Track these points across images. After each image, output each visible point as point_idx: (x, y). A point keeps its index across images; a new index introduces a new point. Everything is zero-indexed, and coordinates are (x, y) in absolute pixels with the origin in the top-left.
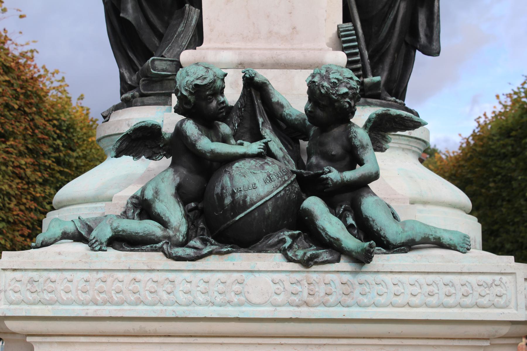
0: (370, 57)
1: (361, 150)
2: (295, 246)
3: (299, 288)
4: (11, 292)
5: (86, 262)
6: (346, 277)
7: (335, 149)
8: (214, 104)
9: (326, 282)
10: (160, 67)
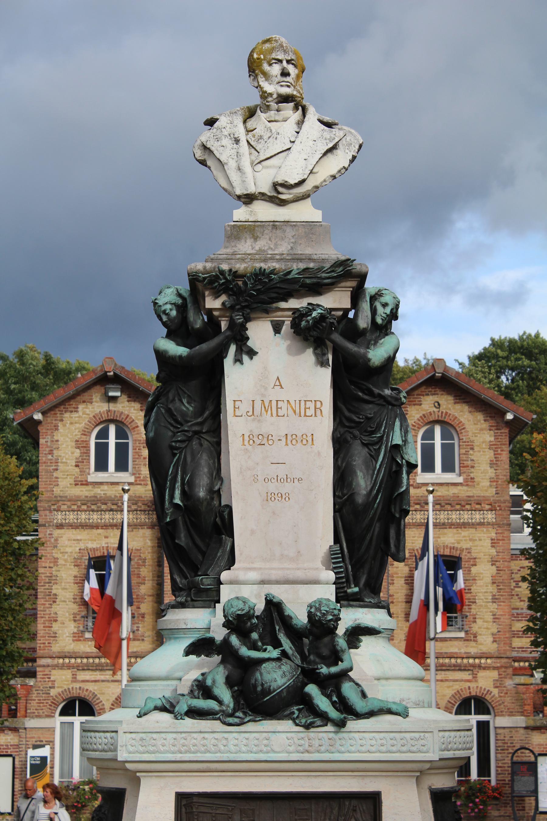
3: (302, 742)
4: (130, 746)
6: (331, 735)
7: (325, 652)
8: (249, 624)
9: (319, 738)
10: (206, 583)
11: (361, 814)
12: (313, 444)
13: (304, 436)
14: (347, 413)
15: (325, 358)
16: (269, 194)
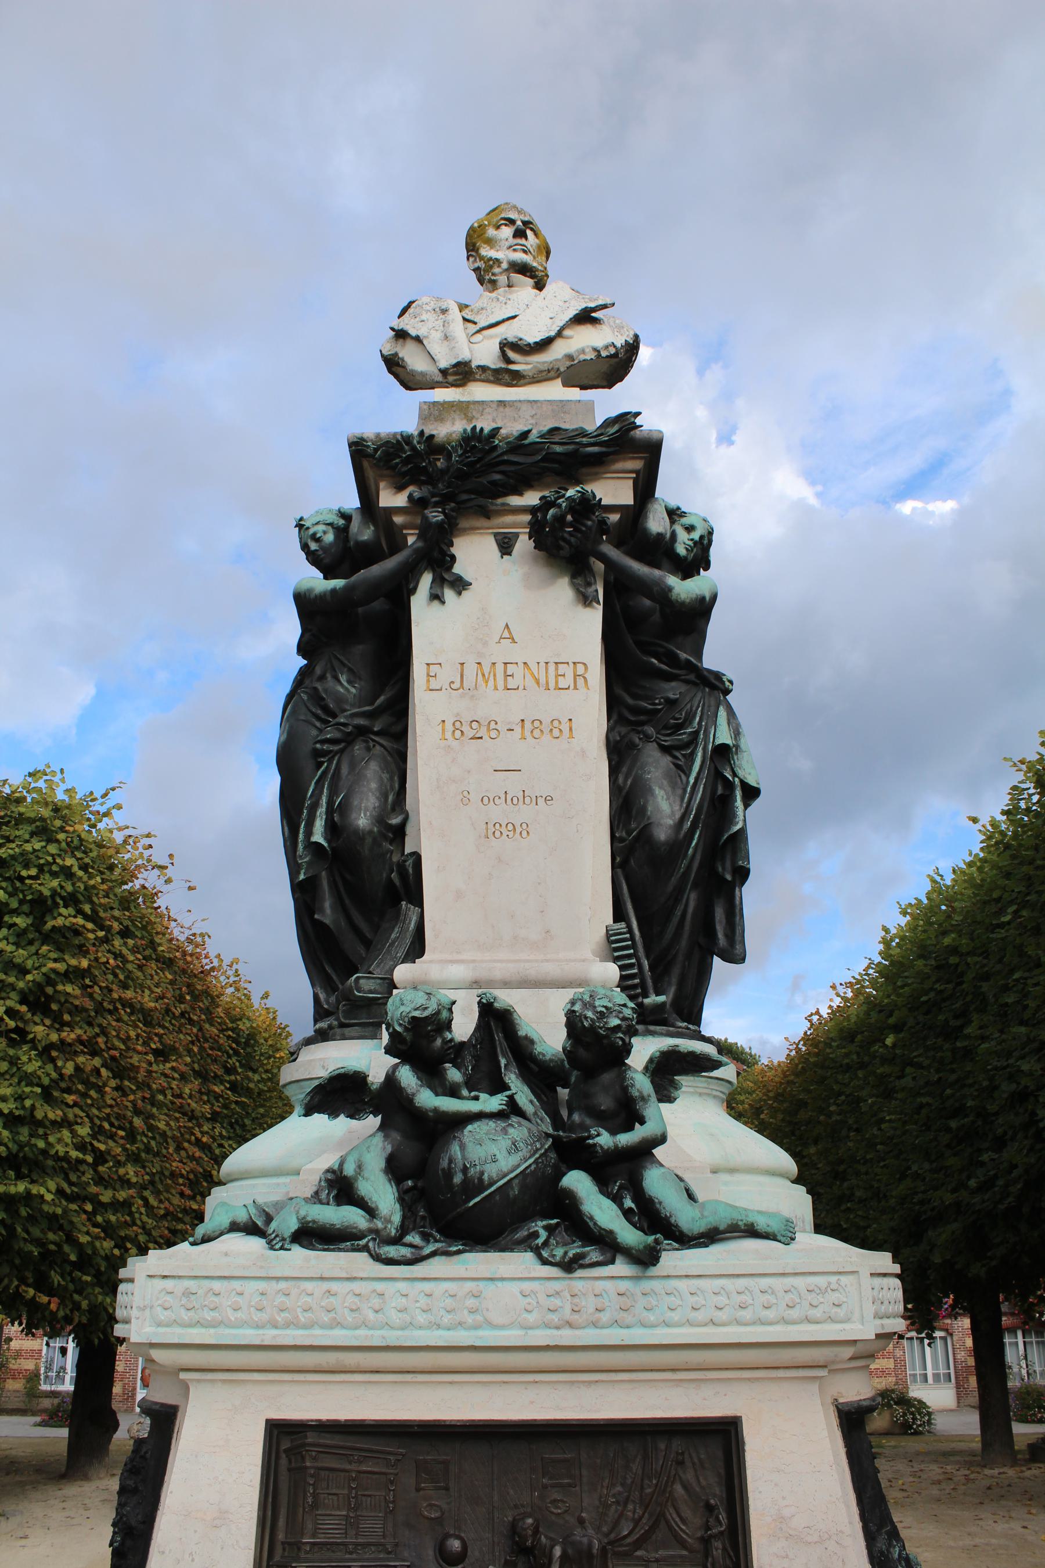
0: (652, 968)
1: (641, 1103)
2: (552, 1241)
3: (558, 1302)
5: (262, 1267)
6: (624, 1285)
8: (439, 1042)
9: (597, 1292)
10: (366, 988)
11: (695, 1470)
13: (556, 723)
14: (630, 701)
15: (591, 590)
16: (493, 367)
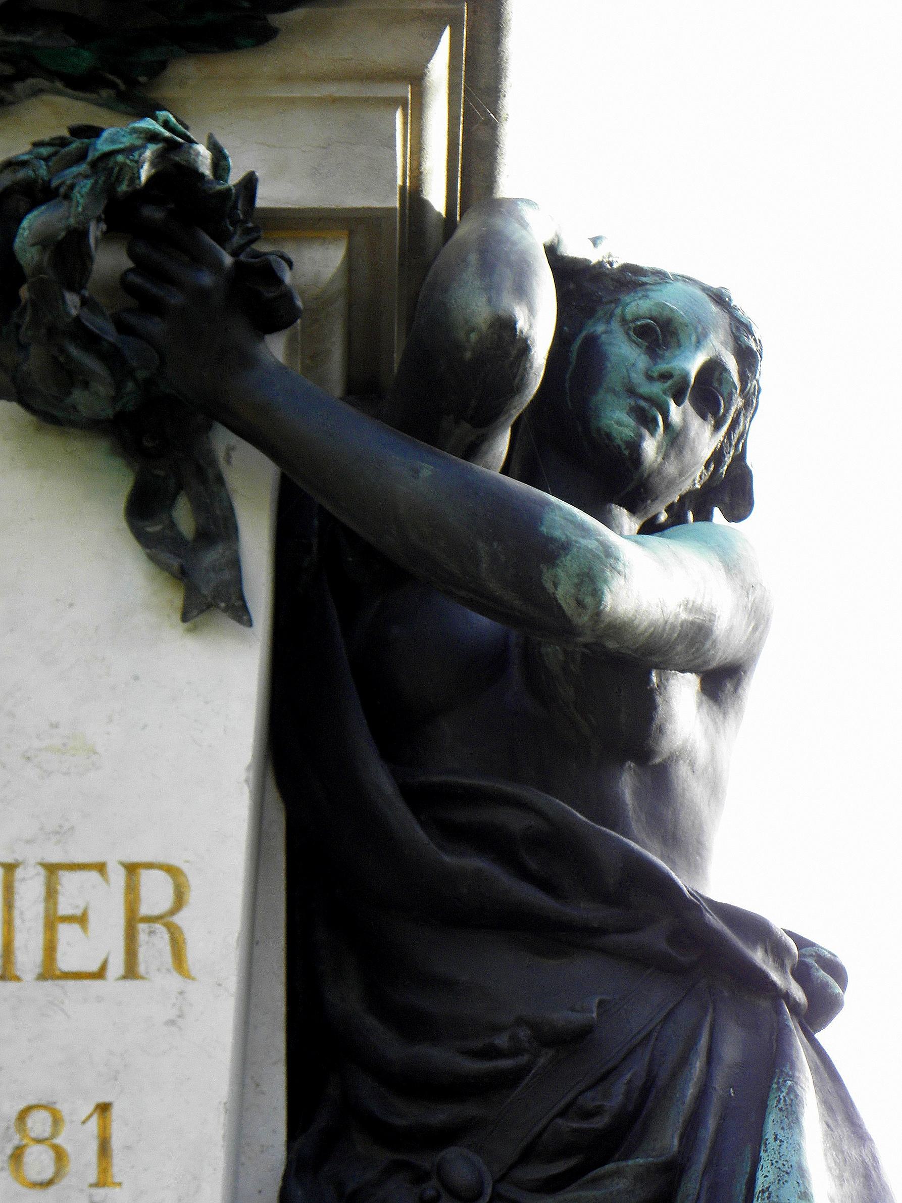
12: (103, 1180)
